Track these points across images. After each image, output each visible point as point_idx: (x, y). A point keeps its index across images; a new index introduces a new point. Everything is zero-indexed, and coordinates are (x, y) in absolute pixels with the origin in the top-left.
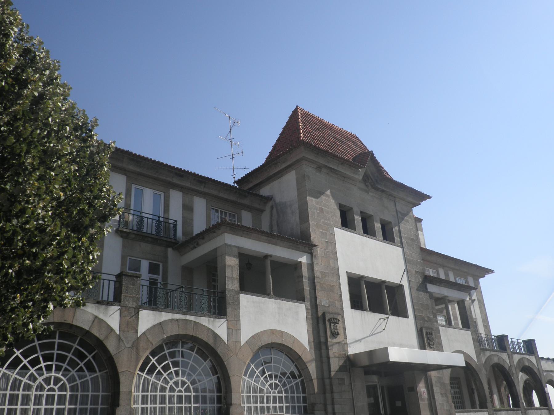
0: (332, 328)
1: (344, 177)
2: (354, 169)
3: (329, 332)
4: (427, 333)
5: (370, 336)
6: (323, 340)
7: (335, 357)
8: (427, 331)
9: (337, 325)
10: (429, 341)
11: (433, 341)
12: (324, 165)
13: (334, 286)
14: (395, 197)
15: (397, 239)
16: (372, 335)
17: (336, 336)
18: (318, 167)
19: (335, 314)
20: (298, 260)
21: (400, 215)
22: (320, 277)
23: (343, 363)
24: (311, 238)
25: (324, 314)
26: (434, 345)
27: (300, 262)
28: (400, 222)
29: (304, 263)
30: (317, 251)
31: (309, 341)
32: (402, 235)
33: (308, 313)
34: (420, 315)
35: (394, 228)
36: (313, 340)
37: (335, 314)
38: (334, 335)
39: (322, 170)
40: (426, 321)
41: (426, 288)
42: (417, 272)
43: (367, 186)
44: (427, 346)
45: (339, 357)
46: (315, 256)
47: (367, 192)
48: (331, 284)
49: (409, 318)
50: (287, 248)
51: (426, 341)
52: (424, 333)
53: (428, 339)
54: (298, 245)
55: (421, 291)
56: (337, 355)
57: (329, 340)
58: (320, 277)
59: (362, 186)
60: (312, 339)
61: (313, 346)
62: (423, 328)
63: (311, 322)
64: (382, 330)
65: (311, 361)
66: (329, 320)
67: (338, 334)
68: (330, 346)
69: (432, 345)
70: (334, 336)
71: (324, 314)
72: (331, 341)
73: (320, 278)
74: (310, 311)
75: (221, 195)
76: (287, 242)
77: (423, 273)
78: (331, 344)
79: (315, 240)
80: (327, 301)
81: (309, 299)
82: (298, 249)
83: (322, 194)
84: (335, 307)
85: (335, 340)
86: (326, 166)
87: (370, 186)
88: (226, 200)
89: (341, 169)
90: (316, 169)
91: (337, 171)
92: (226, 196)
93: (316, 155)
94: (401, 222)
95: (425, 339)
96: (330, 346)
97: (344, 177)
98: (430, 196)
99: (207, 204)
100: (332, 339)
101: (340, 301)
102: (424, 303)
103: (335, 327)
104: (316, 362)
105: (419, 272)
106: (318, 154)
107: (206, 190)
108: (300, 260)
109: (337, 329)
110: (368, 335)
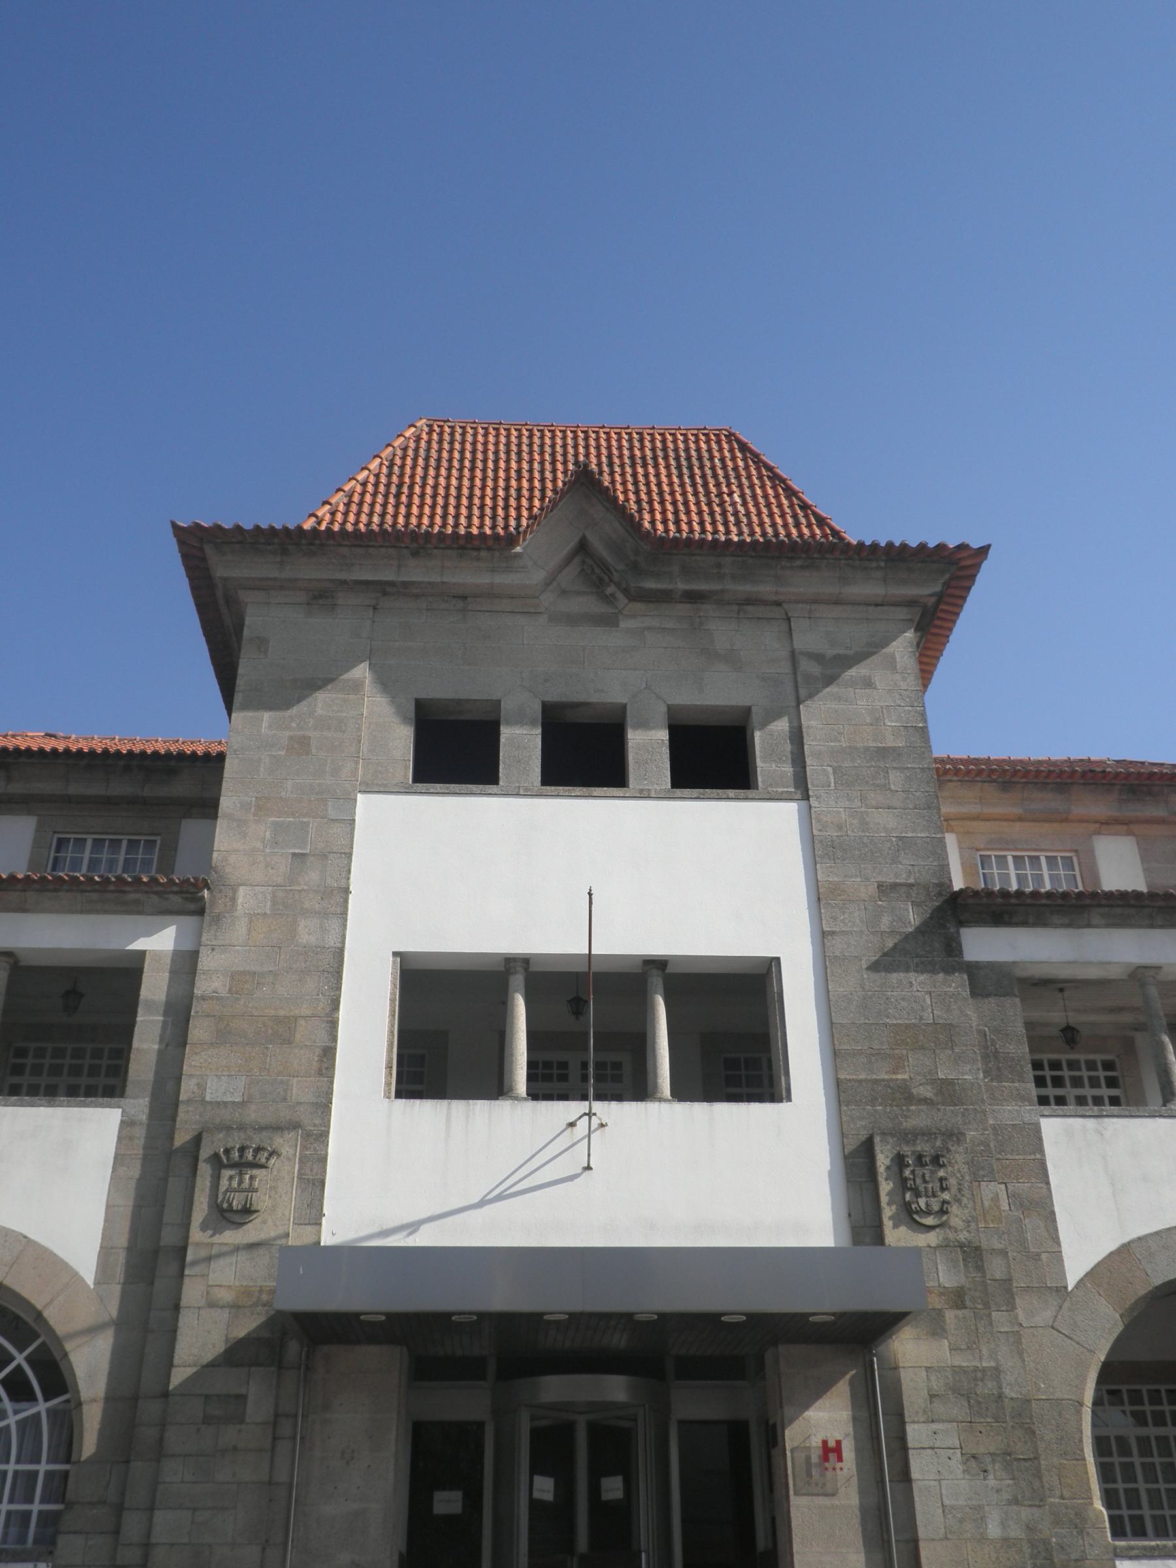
0: (222, 1188)
1: (464, 598)
2: (483, 554)
3: (205, 1206)
4: (899, 1161)
5: (482, 1203)
6: (169, 1237)
7: (212, 1305)
8: (906, 1150)
9: (255, 1172)
10: (908, 1196)
11: (946, 1196)
12: (333, 581)
13: (296, 1018)
14: (778, 604)
15: (764, 766)
16: (500, 1198)
17: (237, 1218)
18: (315, 598)
19: (262, 1129)
20: (127, 948)
21: (805, 665)
22: (224, 993)
23: (260, 1327)
24: (215, 855)
25: (197, 1140)
26: (943, 1212)
27: (142, 953)
28: (802, 696)
29: (158, 954)
30: (234, 899)
31: (105, 1252)
32: (810, 745)
33: (131, 1138)
34: (876, 1081)
35: (763, 725)
36: (125, 1245)
37: (262, 1129)
38: (227, 1215)
39: (340, 602)
40: (925, 1101)
41: (953, 948)
42: (885, 889)
43: (609, 600)
44: (888, 1224)
45: (235, 1307)
46: (217, 919)
47: (609, 621)
48: (282, 1013)
49: (789, 1099)
50: (82, 912)
51: (884, 1199)
52: (883, 1160)
53: (903, 1184)
54: (125, 892)
55: (907, 970)
56: (226, 1296)
57: (196, 1235)
58: (224, 993)
59: (589, 604)
60: (122, 1240)
61: (119, 1272)
62: (877, 1139)
63: (136, 1172)
64: (580, 1171)
65: (93, 1330)
66: (216, 1156)
67: (247, 1211)
68: (194, 1263)
69: (928, 1213)
70: (224, 1218)
71: (197, 1140)
72: (209, 1240)
73: (218, 999)
74: (140, 1133)
75: (74, 789)
76: (68, 891)
77: (941, 885)
78: (203, 1253)
79: (232, 859)
80: (241, 1082)
81: (150, 1088)
82: (135, 909)
83: (319, 688)
84: (285, 1099)
85: (231, 1237)
86: (345, 582)
87: (619, 595)
88: (108, 803)
89: (417, 572)
90: (308, 604)
91: (405, 584)
92: (96, 789)
93: (278, 559)
94: (810, 696)
95: (886, 1187)
96: (194, 1263)
97: (464, 598)
98: (975, 545)
99: (37, 831)
100: (217, 1231)
101: (320, 1073)
102: (921, 1018)
103: (241, 1182)
104: (117, 1336)
105: (911, 886)
106: (285, 552)
107: (17, 788)
108: (138, 945)
109: (252, 1189)
110: (476, 1200)
